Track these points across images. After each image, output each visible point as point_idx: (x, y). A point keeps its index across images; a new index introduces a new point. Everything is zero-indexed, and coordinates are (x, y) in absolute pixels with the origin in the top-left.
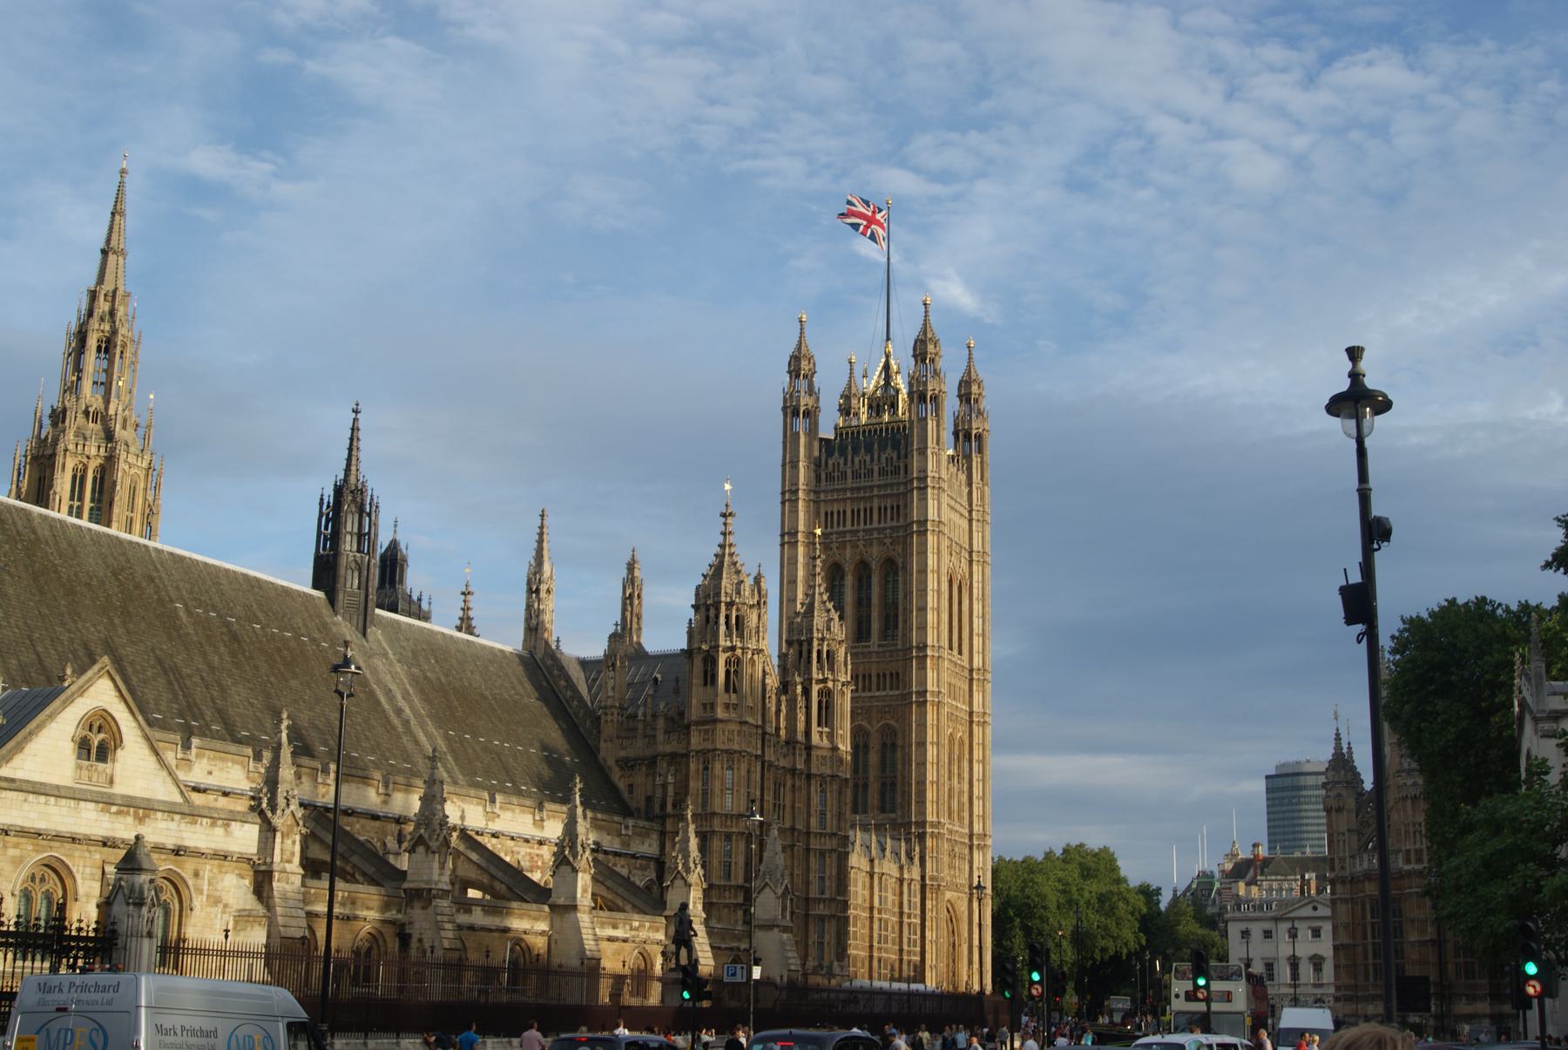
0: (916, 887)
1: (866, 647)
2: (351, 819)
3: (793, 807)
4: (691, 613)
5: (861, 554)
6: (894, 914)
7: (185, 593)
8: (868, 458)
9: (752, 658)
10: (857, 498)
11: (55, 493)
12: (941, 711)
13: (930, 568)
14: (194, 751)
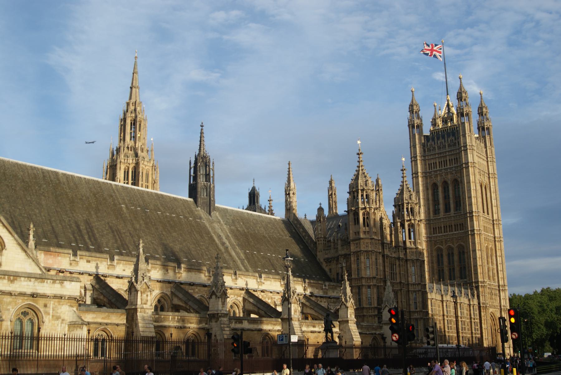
0: (476, 307)
1: (449, 214)
2: (193, 287)
3: (400, 273)
4: (348, 196)
6: (468, 319)
7: (126, 201)
8: (443, 141)
9: (374, 212)
10: (440, 157)
11: (117, 178)
12: (481, 237)
14: (116, 261)
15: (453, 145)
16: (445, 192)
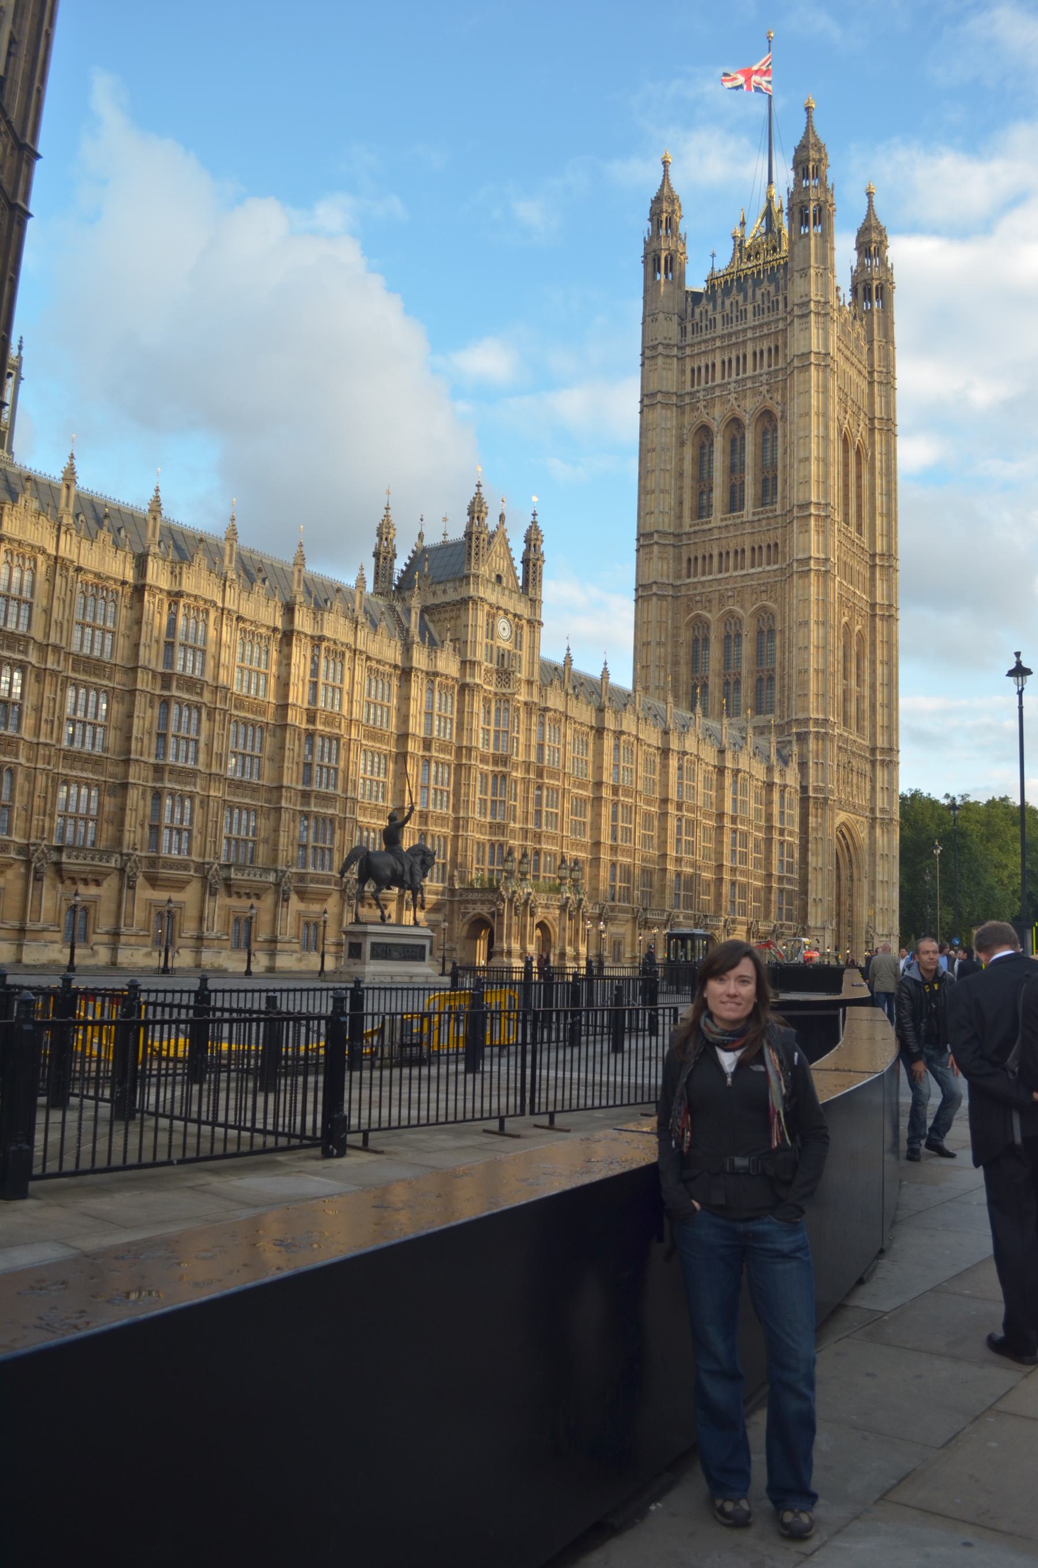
1: (738, 517)
5: (732, 410)
8: (740, 298)
15: (769, 308)
16: (733, 452)
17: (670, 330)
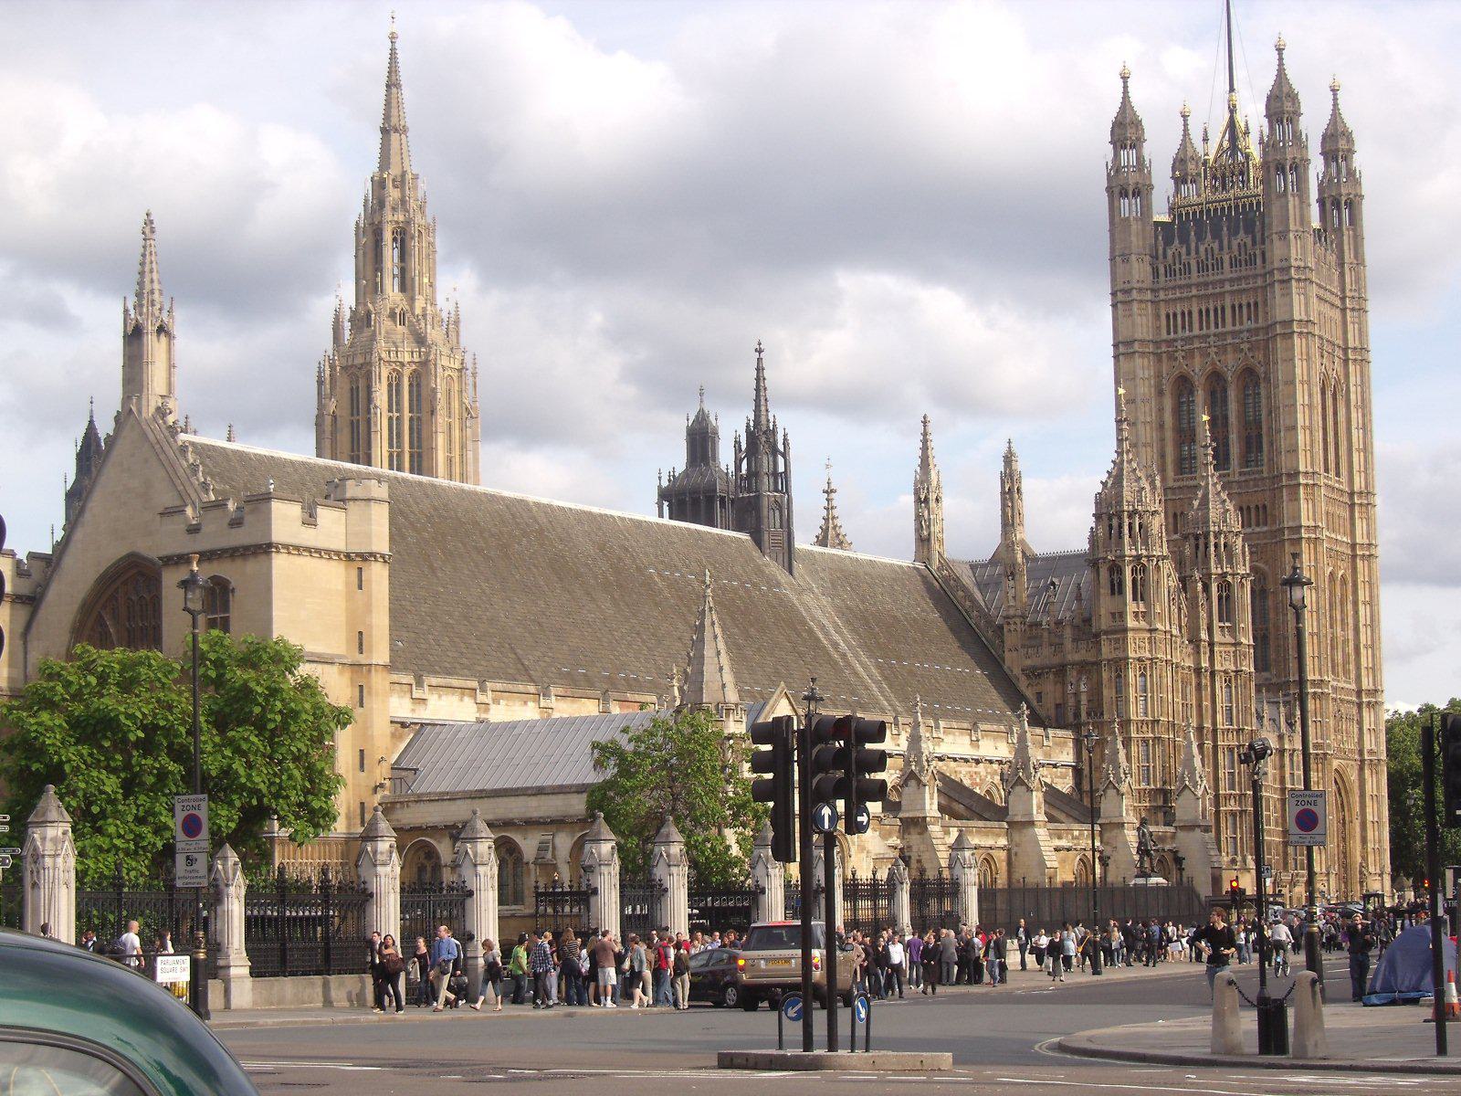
0: (1298, 758)
5: (1213, 364)
8: (1216, 246)
13: (1298, 378)
15: (1246, 261)
17: (1140, 271)
